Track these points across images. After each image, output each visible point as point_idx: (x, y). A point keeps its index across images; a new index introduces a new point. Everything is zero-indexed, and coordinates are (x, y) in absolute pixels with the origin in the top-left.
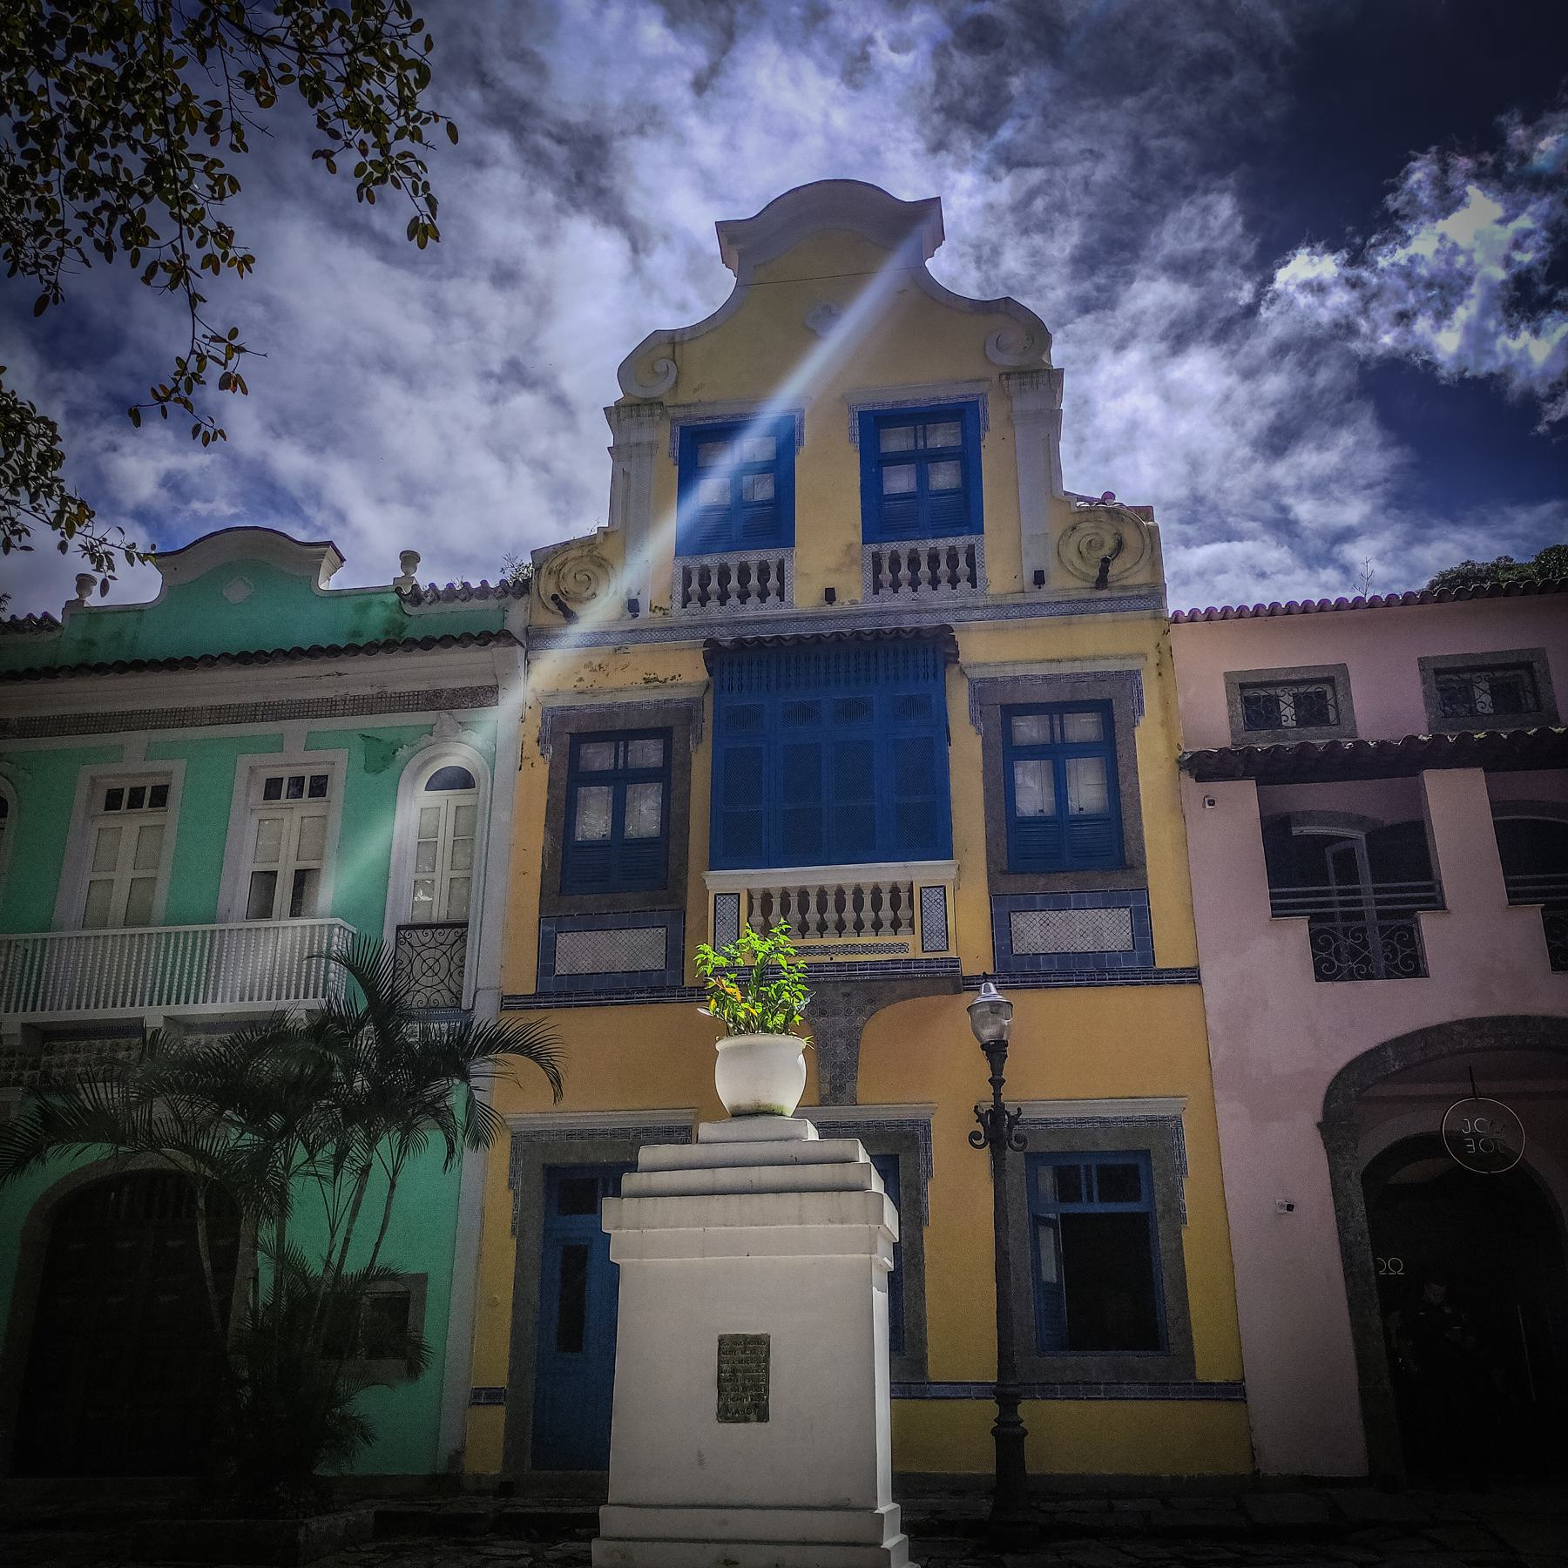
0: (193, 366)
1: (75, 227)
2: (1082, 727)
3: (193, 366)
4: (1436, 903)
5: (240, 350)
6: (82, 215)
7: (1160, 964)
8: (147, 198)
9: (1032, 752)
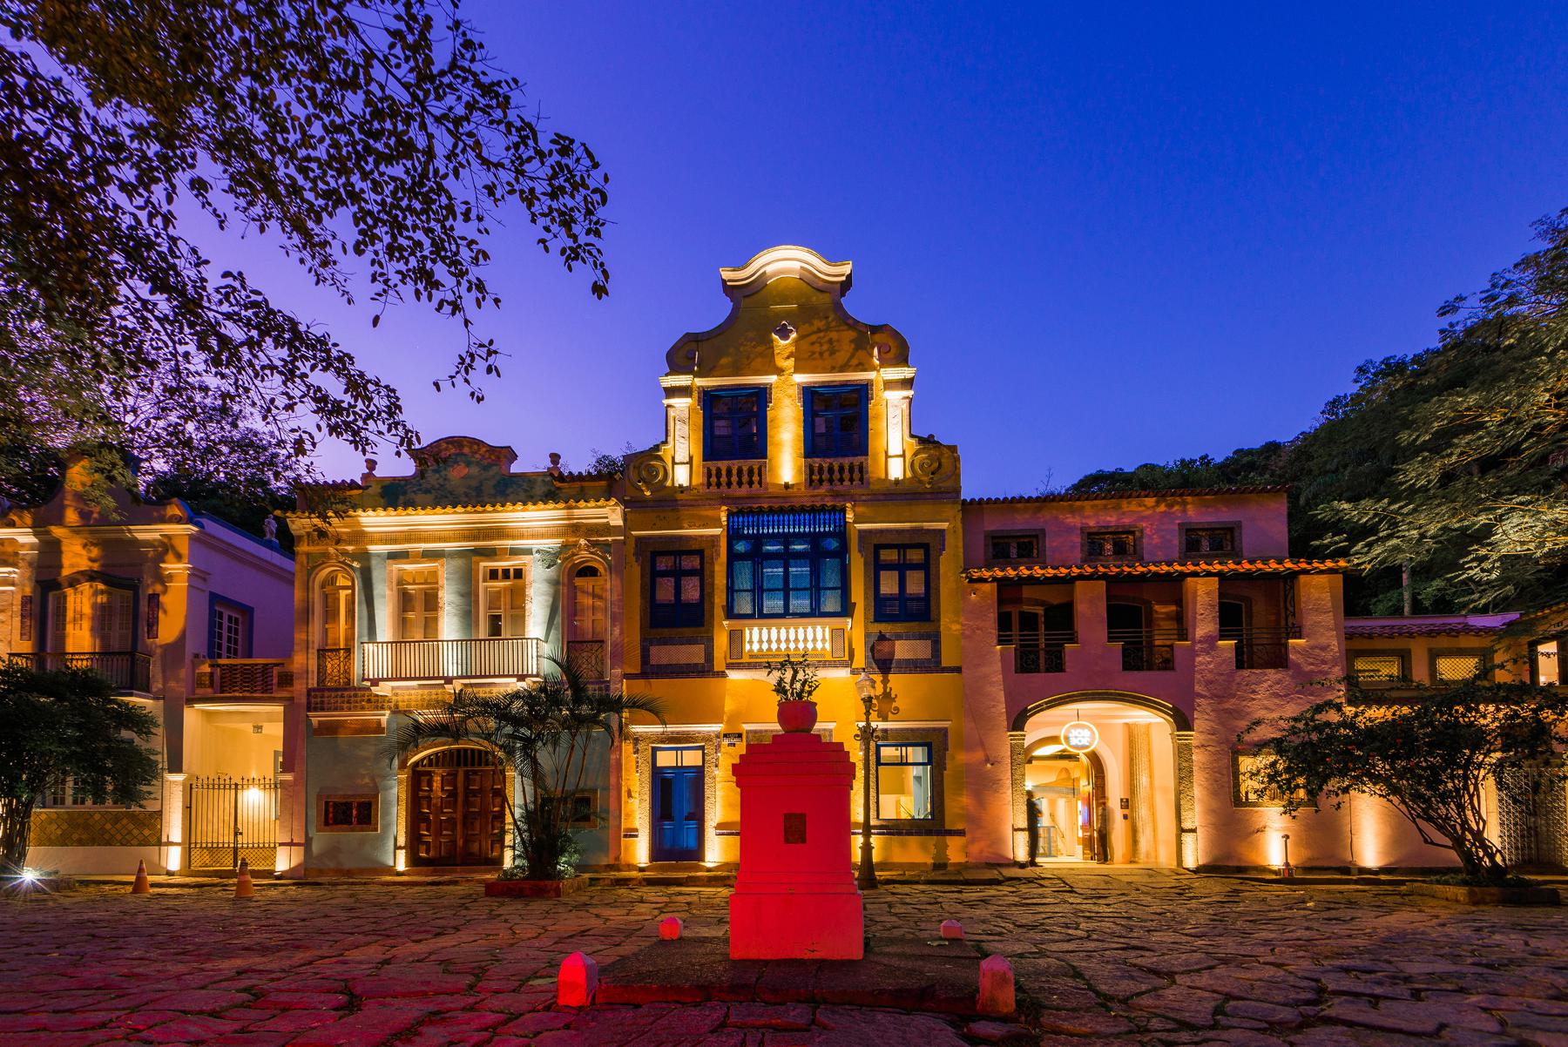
0: (468, 360)
1: (395, 279)
2: (916, 556)
3: (468, 360)
5: (496, 352)
6: (398, 272)
8: (434, 261)
9: (889, 567)
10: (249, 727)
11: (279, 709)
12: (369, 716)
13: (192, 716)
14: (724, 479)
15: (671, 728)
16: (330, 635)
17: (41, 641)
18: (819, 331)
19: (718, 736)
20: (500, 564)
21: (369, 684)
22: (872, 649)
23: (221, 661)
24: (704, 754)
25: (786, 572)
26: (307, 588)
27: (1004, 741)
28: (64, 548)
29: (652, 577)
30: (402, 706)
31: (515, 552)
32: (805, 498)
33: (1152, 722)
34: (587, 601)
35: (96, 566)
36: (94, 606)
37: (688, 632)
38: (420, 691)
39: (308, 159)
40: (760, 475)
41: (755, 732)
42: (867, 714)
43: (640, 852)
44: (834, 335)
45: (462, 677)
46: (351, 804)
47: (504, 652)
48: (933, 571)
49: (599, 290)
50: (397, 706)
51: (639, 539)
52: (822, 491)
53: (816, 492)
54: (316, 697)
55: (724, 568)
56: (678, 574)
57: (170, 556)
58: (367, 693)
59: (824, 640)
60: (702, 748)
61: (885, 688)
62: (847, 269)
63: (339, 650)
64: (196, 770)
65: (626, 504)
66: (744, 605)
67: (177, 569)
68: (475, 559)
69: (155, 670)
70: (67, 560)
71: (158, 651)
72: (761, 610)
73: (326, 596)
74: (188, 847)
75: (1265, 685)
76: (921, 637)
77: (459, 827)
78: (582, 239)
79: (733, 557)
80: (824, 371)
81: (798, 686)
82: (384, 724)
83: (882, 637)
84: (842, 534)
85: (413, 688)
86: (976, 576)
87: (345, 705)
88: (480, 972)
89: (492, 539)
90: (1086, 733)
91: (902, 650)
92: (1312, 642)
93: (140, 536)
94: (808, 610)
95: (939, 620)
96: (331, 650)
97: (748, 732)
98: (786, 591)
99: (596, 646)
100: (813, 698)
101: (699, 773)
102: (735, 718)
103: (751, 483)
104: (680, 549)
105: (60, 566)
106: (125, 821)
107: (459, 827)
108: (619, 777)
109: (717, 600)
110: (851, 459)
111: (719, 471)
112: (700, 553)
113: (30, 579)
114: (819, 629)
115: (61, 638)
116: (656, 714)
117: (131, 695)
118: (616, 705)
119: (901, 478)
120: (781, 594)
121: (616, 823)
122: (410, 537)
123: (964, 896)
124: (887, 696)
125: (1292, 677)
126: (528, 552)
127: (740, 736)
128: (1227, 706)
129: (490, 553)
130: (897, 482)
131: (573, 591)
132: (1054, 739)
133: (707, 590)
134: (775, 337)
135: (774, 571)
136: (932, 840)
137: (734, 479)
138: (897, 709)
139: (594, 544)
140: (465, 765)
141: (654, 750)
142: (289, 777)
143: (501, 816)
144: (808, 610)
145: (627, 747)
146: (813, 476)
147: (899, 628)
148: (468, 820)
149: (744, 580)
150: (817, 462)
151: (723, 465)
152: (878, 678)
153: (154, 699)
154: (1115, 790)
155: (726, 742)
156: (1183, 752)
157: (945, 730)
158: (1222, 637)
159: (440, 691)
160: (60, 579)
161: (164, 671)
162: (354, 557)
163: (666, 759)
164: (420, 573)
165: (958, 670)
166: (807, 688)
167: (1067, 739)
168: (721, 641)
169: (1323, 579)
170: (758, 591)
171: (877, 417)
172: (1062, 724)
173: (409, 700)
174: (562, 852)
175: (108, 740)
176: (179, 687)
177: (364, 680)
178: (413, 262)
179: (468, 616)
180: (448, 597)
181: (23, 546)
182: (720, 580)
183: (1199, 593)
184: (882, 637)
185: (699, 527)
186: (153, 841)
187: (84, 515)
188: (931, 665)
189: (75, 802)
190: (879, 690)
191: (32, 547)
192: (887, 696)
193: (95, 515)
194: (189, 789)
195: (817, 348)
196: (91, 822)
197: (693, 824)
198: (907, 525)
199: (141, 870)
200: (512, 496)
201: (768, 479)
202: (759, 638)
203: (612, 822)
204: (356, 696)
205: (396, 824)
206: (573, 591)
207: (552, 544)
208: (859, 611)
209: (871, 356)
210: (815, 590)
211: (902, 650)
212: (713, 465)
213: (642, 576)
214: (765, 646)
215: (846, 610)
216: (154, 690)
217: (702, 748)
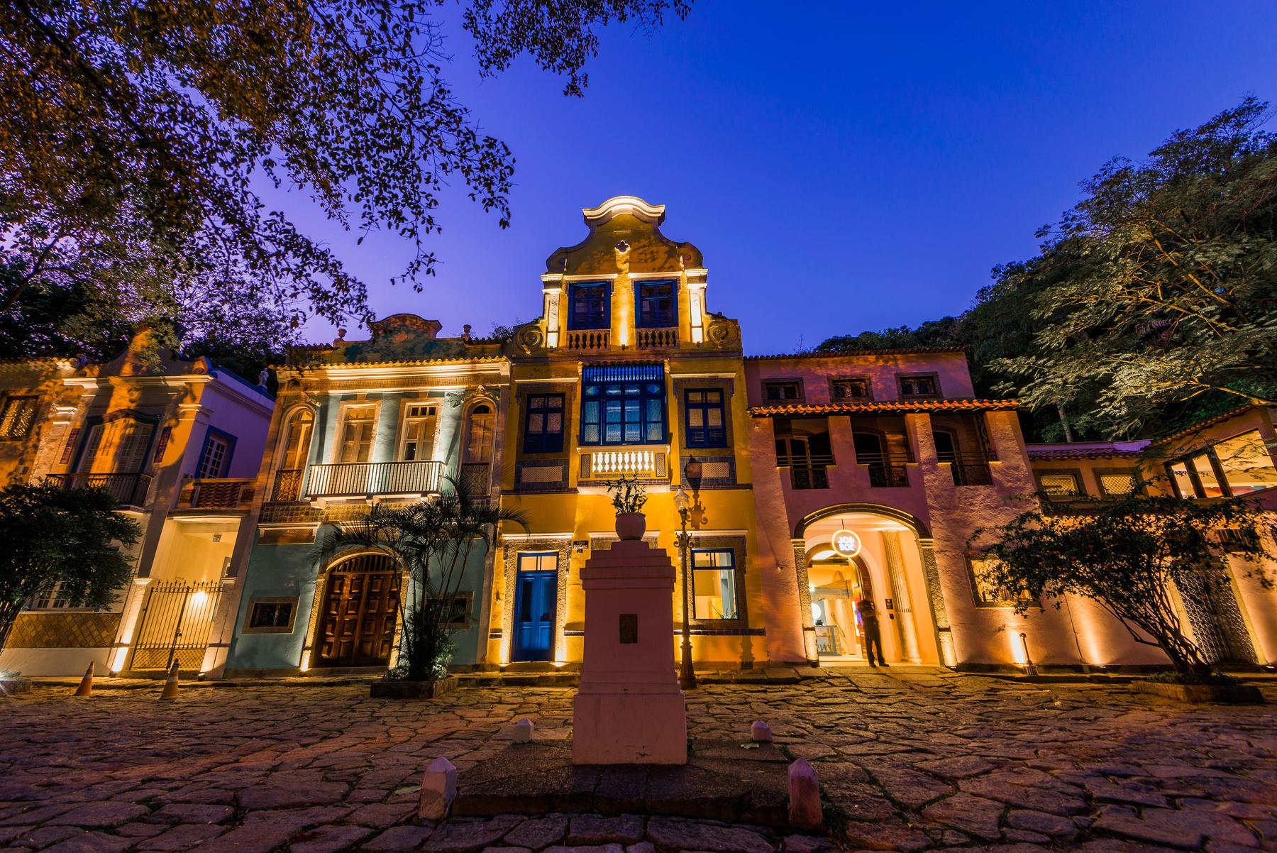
0: (416, 266)
1: (377, 216)
2: (714, 397)
3: (416, 266)
4: (832, 462)
7: (739, 482)
8: (403, 206)
9: (696, 405)
10: (210, 536)
11: (237, 520)
15: (534, 537)
17: (73, 468)
20: (420, 404)
21: (309, 499)
23: (203, 481)
25: (623, 410)
26: (279, 422)
28: (114, 392)
29: (528, 412)
30: (331, 518)
31: (432, 395)
34: (479, 432)
35: (133, 406)
36: (122, 437)
37: (551, 456)
38: (347, 505)
39: (338, 149)
42: (684, 523)
43: (502, 652)
45: (378, 494)
47: (412, 474)
48: (726, 409)
49: (504, 224)
50: (327, 518)
51: (520, 385)
53: (643, 352)
54: (267, 510)
56: (546, 411)
57: (188, 398)
59: (650, 462)
62: (662, 209)
64: (160, 575)
65: (513, 360)
66: (593, 435)
67: (190, 408)
68: (402, 400)
69: (152, 488)
70: (112, 403)
71: (159, 472)
72: (604, 439)
73: (292, 428)
74: (135, 647)
76: (721, 460)
78: (497, 194)
79: (585, 398)
81: (631, 500)
83: (692, 460)
85: (342, 503)
86: (757, 412)
88: (354, 780)
89: (417, 385)
93: (171, 384)
94: (638, 439)
98: (623, 424)
99: (482, 468)
100: (642, 511)
104: (547, 392)
105: (107, 406)
106: (90, 623)
109: (573, 432)
113: (82, 416)
114: (646, 453)
115: (90, 462)
116: (523, 523)
117: (128, 509)
118: (492, 517)
120: (619, 426)
121: (485, 624)
123: (769, 696)
126: (442, 395)
129: (414, 396)
131: (470, 424)
133: (566, 423)
136: (739, 639)
139: (488, 389)
143: (393, 618)
144: (638, 439)
149: (593, 416)
153: (144, 512)
159: (362, 505)
160: (104, 416)
161: (158, 489)
164: (362, 410)
166: (638, 502)
168: (575, 463)
170: (603, 423)
173: (337, 513)
174: (438, 654)
175: (100, 547)
176: (166, 502)
177: (306, 496)
178: (390, 206)
179: (392, 444)
180: (380, 430)
181: (86, 391)
182: (576, 416)
184: (692, 460)
186: (108, 641)
187: (136, 369)
188: (729, 483)
189: (55, 605)
190: (692, 504)
191: (92, 391)
193: (144, 369)
196: (62, 624)
197: (546, 624)
199: (89, 671)
202: (603, 461)
203: (482, 624)
204: (298, 509)
205: (307, 629)
206: (470, 424)
207: (458, 389)
208: (675, 439)
210: (644, 423)
214: (607, 468)
215: (666, 439)
216: (147, 504)
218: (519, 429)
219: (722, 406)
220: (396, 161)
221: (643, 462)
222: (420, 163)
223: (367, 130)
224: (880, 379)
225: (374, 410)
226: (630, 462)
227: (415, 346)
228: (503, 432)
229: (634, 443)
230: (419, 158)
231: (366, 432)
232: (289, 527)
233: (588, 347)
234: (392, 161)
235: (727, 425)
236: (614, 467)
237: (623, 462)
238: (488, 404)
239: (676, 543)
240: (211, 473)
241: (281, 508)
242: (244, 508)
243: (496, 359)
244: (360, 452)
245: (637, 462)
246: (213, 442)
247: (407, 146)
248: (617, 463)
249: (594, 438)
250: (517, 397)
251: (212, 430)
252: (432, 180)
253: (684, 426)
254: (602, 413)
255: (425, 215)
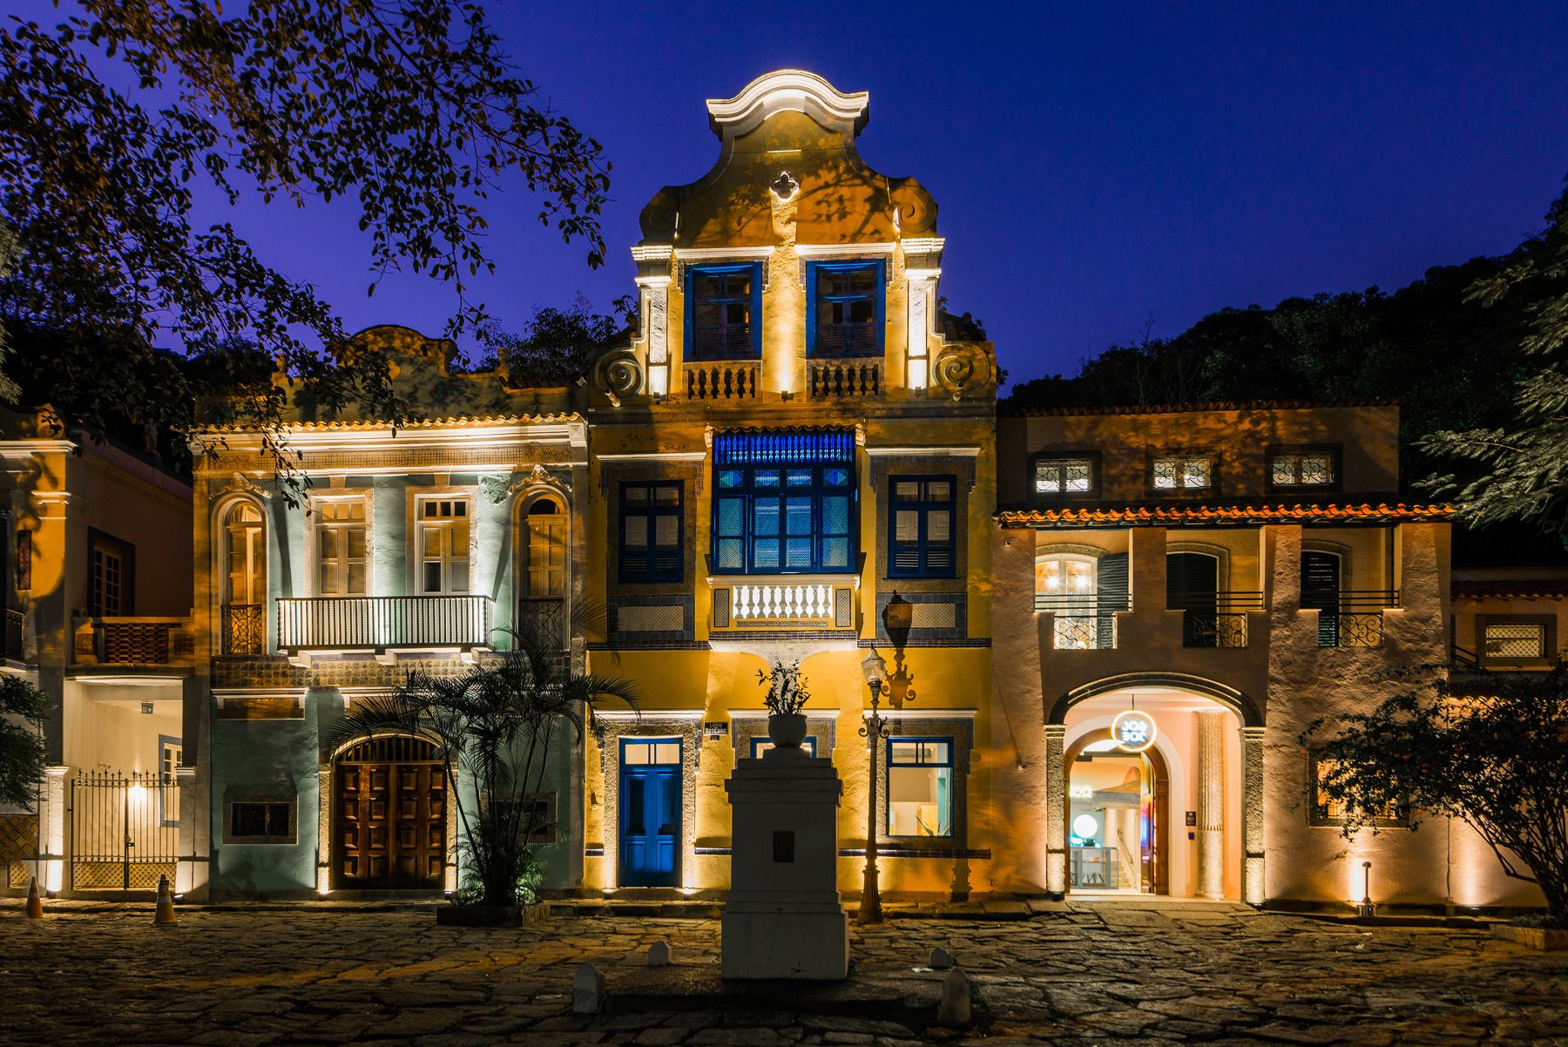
2: (939, 490)
9: (908, 505)
11: (176, 683)
12: (284, 694)
13: (71, 690)
14: (708, 387)
16: (236, 587)
18: (827, 185)
19: (699, 727)
20: (439, 497)
21: (285, 652)
22: (885, 615)
23: (107, 620)
24: (681, 750)
25: (783, 514)
26: (208, 526)
27: (1039, 737)
30: (324, 681)
31: (456, 481)
32: (805, 413)
33: (1219, 711)
34: (540, 546)
37: (664, 589)
38: (345, 663)
40: (752, 381)
41: (743, 721)
44: (845, 192)
45: (391, 646)
46: (263, 807)
47: (442, 616)
48: (959, 512)
50: (317, 681)
51: (605, 464)
52: (827, 404)
54: (221, 668)
55: (709, 503)
58: (282, 663)
59: (826, 602)
60: (680, 741)
61: (899, 665)
63: (247, 606)
65: (590, 418)
66: (731, 556)
68: (408, 489)
69: (28, 630)
71: (32, 605)
72: (751, 562)
75: (1353, 667)
76: (944, 599)
77: (391, 839)
79: (719, 493)
80: (832, 240)
82: (302, 705)
83: (897, 599)
84: (851, 467)
85: (336, 658)
86: (1011, 519)
87: (256, 679)
89: (430, 463)
90: (1142, 726)
91: (922, 616)
92: (1412, 612)
94: (807, 564)
95: (966, 578)
96: (238, 607)
97: (734, 721)
98: (782, 537)
99: (553, 606)
101: (676, 771)
102: (720, 703)
103: (741, 392)
104: (653, 477)
107: (391, 839)
108: (581, 777)
109: (699, 548)
110: (864, 360)
111: (702, 374)
112: (679, 484)
114: (821, 589)
119: (923, 387)
120: (776, 542)
122: (331, 459)
124: (901, 677)
125: (1386, 657)
126: (472, 481)
127: (725, 726)
128: (1306, 694)
129: (427, 482)
130: (918, 391)
131: (526, 532)
132: (1103, 733)
133: (688, 533)
134: (773, 193)
135: (767, 510)
137: (722, 386)
138: (912, 693)
139: (552, 471)
140: (399, 759)
141: (623, 743)
142: (190, 772)
144: (807, 564)
145: (590, 741)
146: (819, 385)
147: (916, 587)
148: (402, 830)
149: (732, 523)
150: (821, 363)
151: (707, 366)
152: (888, 654)
153: (27, 669)
154: (1180, 802)
155: (708, 734)
156: (1252, 754)
157: (970, 721)
158: (1305, 603)
159: (368, 662)
161: (39, 631)
162: (264, 484)
163: (636, 755)
164: (343, 506)
165: (987, 643)
167: (1119, 732)
168: (703, 601)
169: (1428, 529)
170: (748, 538)
171: (896, 304)
172: (1116, 712)
173: (332, 674)
176: (56, 654)
177: (280, 647)
179: (402, 565)
180: (378, 540)
182: (703, 521)
183: (1279, 545)
184: (897, 599)
185: (678, 450)
192: (901, 677)
194: (70, 785)
195: (824, 209)
198: (930, 451)
200: (452, 408)
201: (762, 386)
202: (748, 599)
204: (268, 667)
206: (526, 532)
207: (503, 470)
208: (870, 565)
209: (890, 220)
210: (818, 536)
211: (922, 616)
212: (695, 366)
213: (610, 514)
214: (756, 611)
215: (855, 564)
216: (27, 657)
217: (680, 741)
218: (610, 543)
219: (952, 505)
220: (414, 152)
221: (815, 603)
222: (452, 150)
223: (363, 98)
224: (1240, 455)
225: (361, 506)
226: (794, 603)
227: (416, 389)
228: (582, 547)
229: (802, 571)
230: (448, 144)
231: (355, 545)
232: (264, 695)
233: (722, 396)
234: (408, 152)
235: (959, 539)
236: (767, 611)
237: (783, 602)
238: (553, 498)
239: (862, 730)
240: (108, 605)
241: (242, 664)
242: (180, 664)
243: (563, 417)
244: (350, 578)
245: (804, 603)
246: (99, 554)
247: (428, 119)
248: (772, 603)
249: (735, 562)
250: (601, 485)
251: (94, 535)
252: (471, 180)
253: (885, 540)
254: (748, 516)
255: (467, 242)
